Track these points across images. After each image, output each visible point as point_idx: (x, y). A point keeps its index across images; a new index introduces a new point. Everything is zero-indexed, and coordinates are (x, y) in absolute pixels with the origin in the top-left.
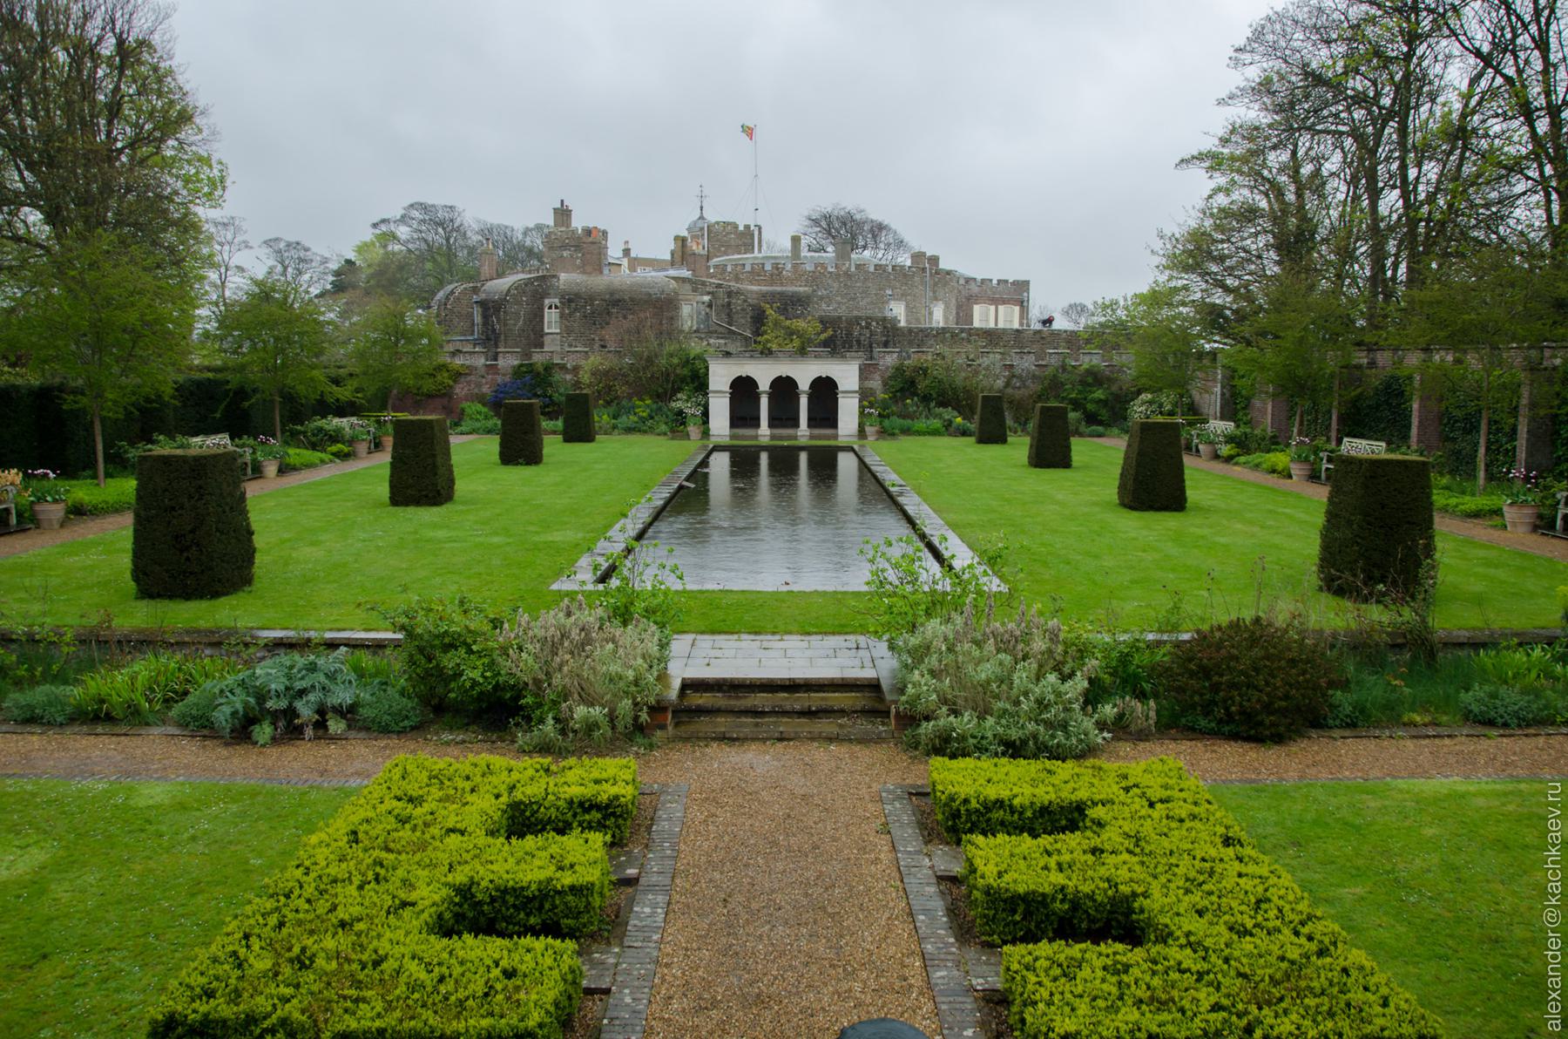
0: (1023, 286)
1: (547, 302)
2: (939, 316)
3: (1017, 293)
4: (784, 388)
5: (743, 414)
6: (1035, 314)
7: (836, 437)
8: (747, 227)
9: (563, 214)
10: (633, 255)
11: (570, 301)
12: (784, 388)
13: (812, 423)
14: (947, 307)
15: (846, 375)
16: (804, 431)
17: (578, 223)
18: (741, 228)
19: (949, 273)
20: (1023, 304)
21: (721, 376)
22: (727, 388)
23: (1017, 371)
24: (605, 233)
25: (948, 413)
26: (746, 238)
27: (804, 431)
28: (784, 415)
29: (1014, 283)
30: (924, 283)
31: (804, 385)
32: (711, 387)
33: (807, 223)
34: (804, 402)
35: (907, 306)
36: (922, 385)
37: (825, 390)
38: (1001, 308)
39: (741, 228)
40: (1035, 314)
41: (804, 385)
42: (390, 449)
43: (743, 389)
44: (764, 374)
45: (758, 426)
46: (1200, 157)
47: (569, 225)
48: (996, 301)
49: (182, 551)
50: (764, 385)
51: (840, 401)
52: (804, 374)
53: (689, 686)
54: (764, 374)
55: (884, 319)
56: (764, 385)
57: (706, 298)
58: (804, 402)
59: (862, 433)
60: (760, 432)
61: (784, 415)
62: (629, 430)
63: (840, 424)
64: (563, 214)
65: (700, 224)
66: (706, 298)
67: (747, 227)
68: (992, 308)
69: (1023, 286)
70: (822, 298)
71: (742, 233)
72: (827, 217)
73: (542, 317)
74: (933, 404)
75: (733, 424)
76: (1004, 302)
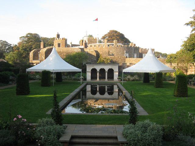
4: (102, 71)
5: (94, 77)
8: (96, 38)
12: (102, 71)
13: (108, 78)
18: (95, 38)
22: (90, 71)
24: (67, 39)
28: (102, 77)
34: (106, 74)
35: (129, 54)
37: (111, 71)
43: (94, 71)
50: (98, 70)
53: (73, 137)
54: (98, 68)
56: (98, 70)
58: (106, 74)
61: (102, 77)
67: (96, 38)
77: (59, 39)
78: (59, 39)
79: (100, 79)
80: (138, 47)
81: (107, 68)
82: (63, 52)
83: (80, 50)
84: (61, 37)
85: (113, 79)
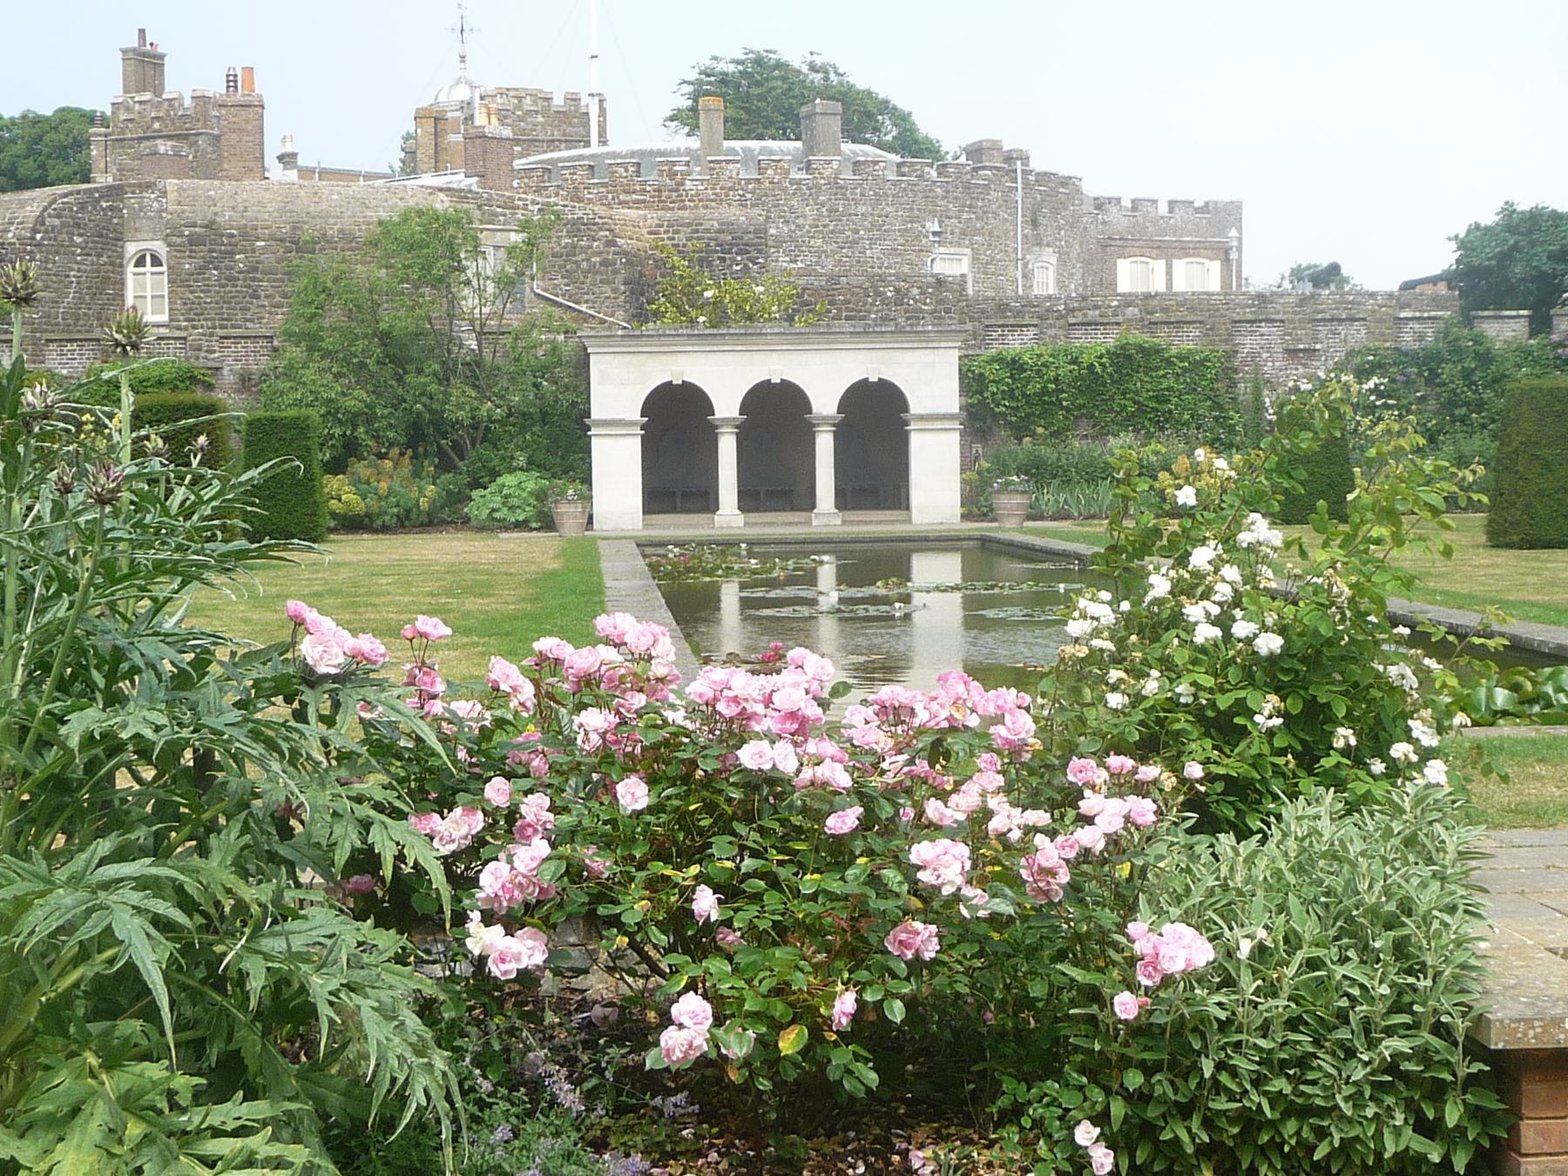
1: (132, 249)
2: (1045, 280)
3: (1213, 229)
4: (776, 409)
5: (675, 476)
7: (910, 521)
8: (573, 99)
9: (145, 65)
10: (302, 161)
11: (193, 241)
12: (776, 409)
14: (1062, 262)
17: (189, 78)
18: (558, 101)
19: (1066, 181)
20: (1225, 255)
21: (619, 387)
26: (570, 123)
27: (827, 512)
28: (775, 480)
29: (1205, 209)
30: (1010, 205)
31: (825, 401)
32: (596, 413)
34: (825, 445)
37: (876, 416)
38: (1179, 265)
39: (558, 101)
41: (825, 401)
43: (675, 419)
44: (726, 378)
47: (158, 90)
48: (1168, 250)
50: (727, 405)
51: (916, 441)
52: (825, 377)
54: (726, 378)
55: (940, 282)
56: (727, 405)
57: (515, 238)
60: (718, 518)
61: (775, 480)
64: (145, 65)
66: (515, 238)
68: (1160, 265)
70: (779, 243)
71: (562, 116)
73: (123, 283)
75: (647, 510)
76: (1185, 251)
81: (825, 377)
82: (248, 235)
85: (908, 508)
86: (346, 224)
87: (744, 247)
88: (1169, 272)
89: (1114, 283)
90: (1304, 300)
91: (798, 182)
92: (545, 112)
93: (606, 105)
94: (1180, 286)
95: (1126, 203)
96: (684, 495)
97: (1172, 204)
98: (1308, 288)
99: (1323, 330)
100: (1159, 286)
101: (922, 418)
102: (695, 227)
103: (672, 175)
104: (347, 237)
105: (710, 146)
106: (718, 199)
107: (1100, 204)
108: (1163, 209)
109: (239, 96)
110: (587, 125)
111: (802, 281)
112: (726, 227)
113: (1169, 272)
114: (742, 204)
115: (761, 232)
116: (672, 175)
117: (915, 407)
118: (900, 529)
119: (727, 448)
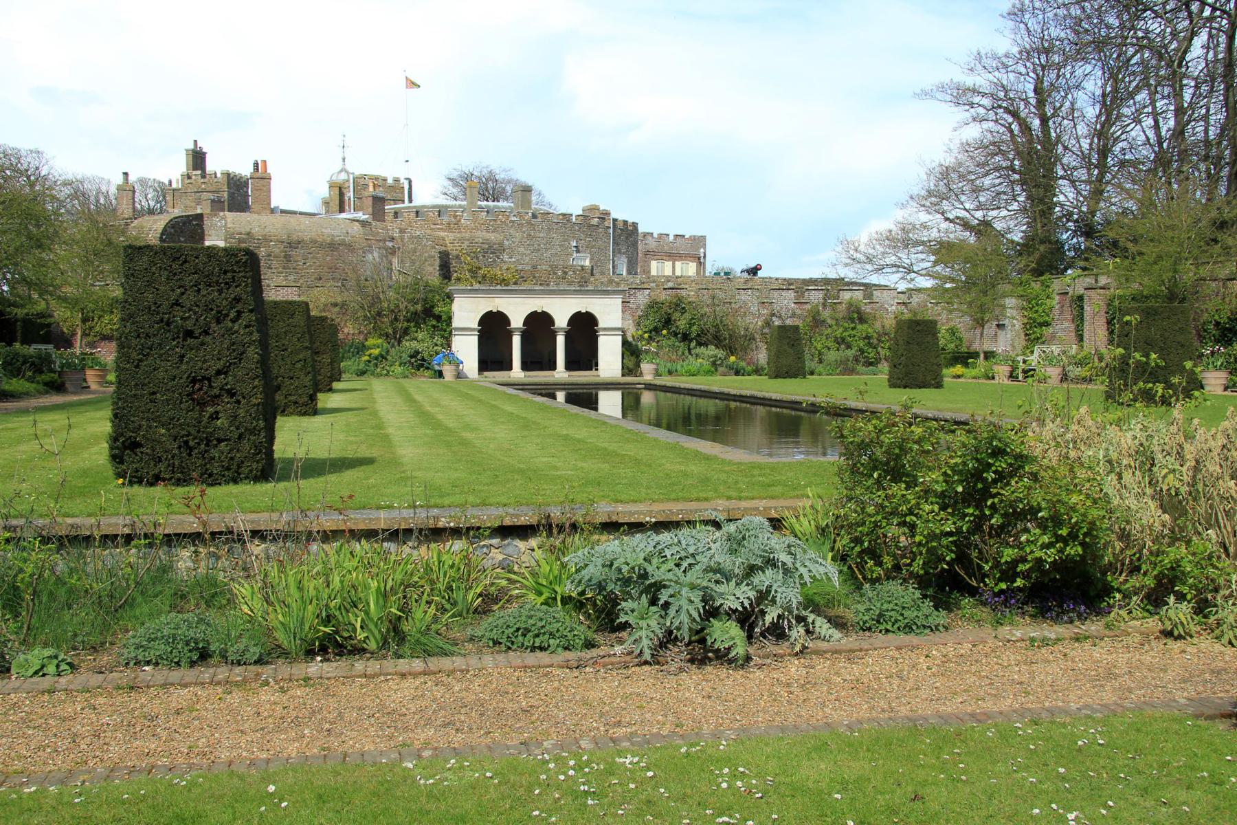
0: (700, 241)
3: (692, 249)
4: (539, 323)
6: (710, 269)
8: (397, 180)
9: (198, 158)
12: (539, 323)
13: (570, 366)
15: (609, 313)
16: (561, 373)
18: (390, 181)
21: (467, 311)
22: (476, 326)
23: (776, 307)
25: (712, 350)
27: (561, 373)
28: (538, 358)
31: (561, 321)
32: (456, 323)
33: (448, 183)
36: (682, 323)
37: (584, 326)
38: (678, 264)
39: (390, 181)
40: (710, 269)
41: (561, 321)
42: (100, 381)
43: (493, 329)
44: (517, 310)
45: (511, 369)
46: (942, 88)
48: (673, 256)
49: (202, 404)
50: (517, 322)
52: (562, 311)
54: (517, 310)
56: (517, 322)
59: (627, 371)
61: (538, 358)
62: (363, 373)
63: (600, 367)
64: (198, 158)
65: (343, 176)
69: (700, 241)
72: (468, 177)
74: (693, 344)
77: (203, 176)
78: (203, 176)
79: (526, 366)
80: (635, 225)
81: (562, 311)
83: (357, 226)
84: (211, 166)
86: (313, 235)
87: (494, 250)
88: (674, 267)
89: (649, 272)
90: (747, 281)
91: (513, 222)
92: (383, 186)
93: (413, 184)
94: (678, 273)
95: (655, 235)
96: (493, 363)
97: (676, 236)
98: (746, 275)
99: (776, 293)
100: (668, 272)
101: (605, 329)
102: (471, 241)
103: (455, 217)
104: (314, 241)
105: (472, 203)
106: (476, 228)
107: (645, 235)
108: (671, 238)
109: (257, 175)
110: (403, 193)
111: (520, 267)
112: (486, 241)
113: (674, 267)
114: (487, 230)
115: (501, 244)
116: (455, 217)
117: (601, 325)
118: (596, 380)
119: (516, 341)
